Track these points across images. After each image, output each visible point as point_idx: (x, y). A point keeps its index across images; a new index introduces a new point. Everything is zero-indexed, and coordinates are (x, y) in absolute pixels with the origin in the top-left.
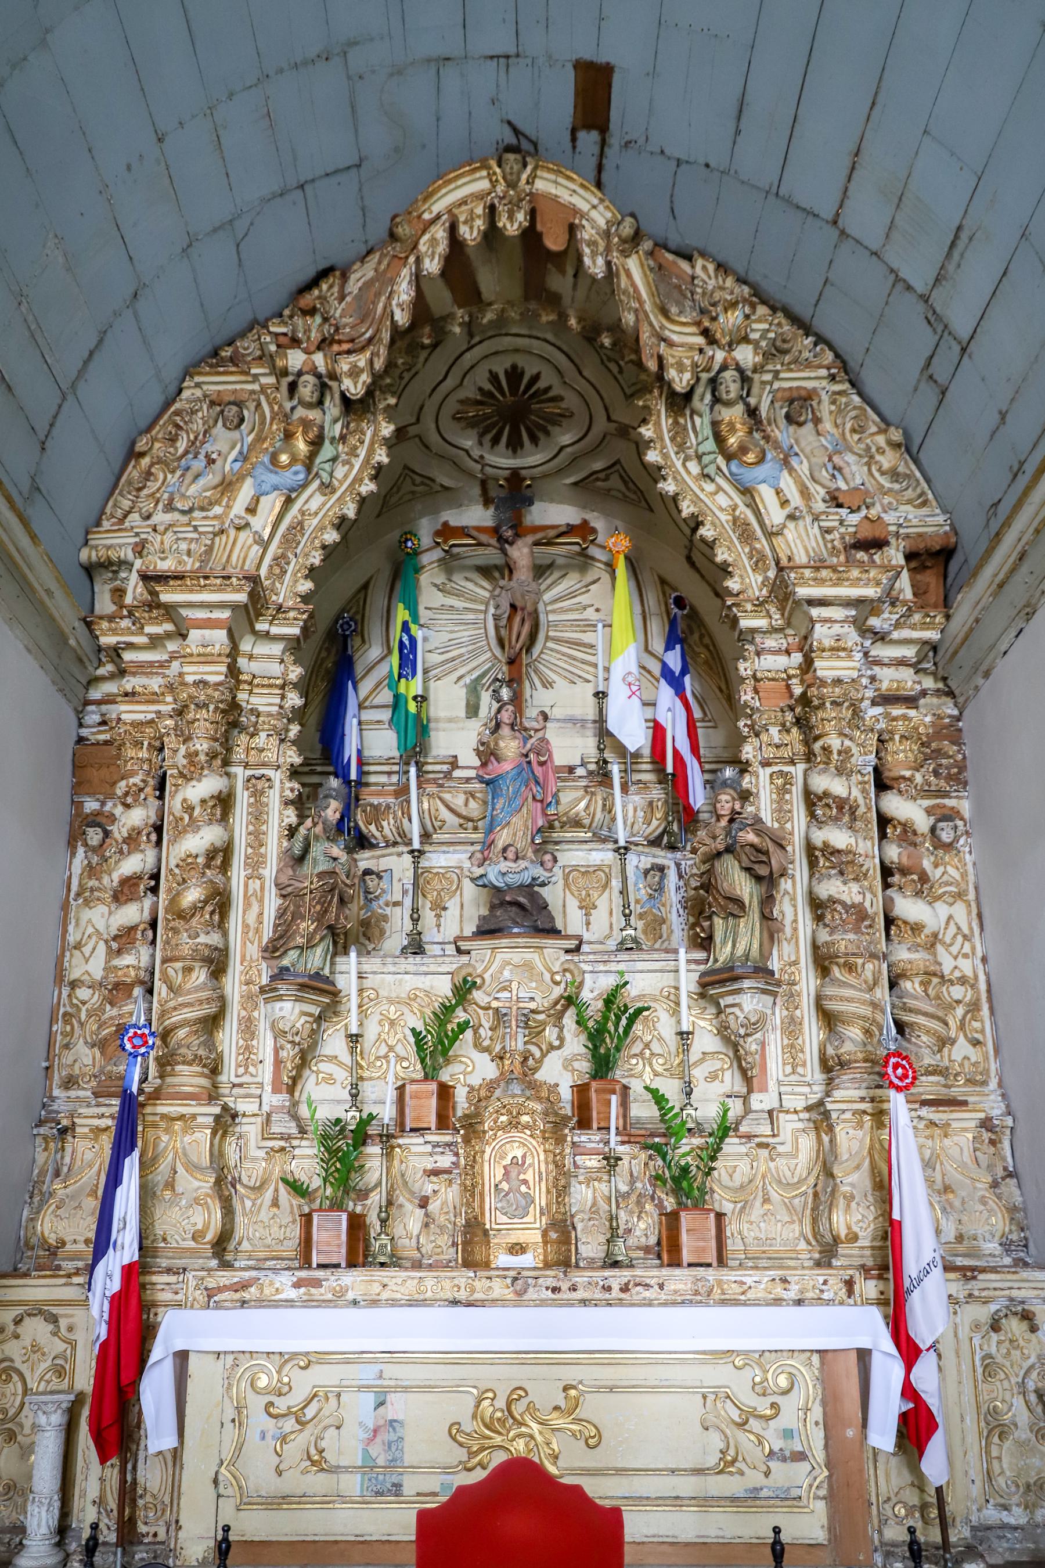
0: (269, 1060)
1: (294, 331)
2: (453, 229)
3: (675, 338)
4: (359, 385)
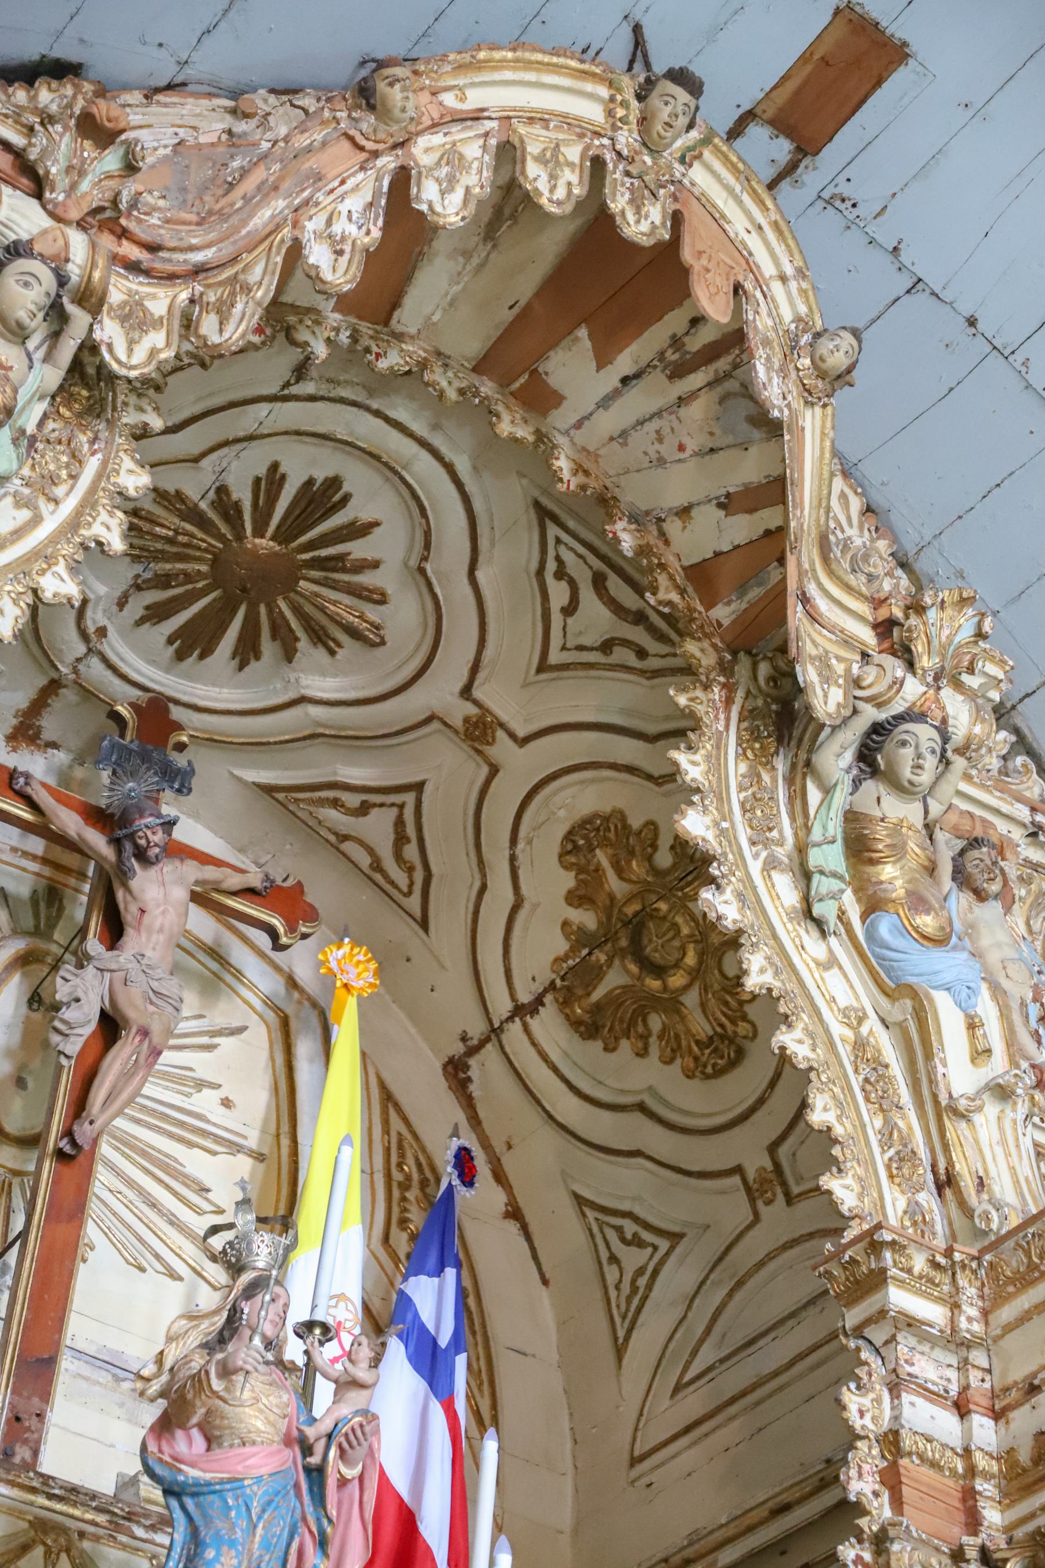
1: (44, 153)
3: (822, 605)
4: (140, 355)
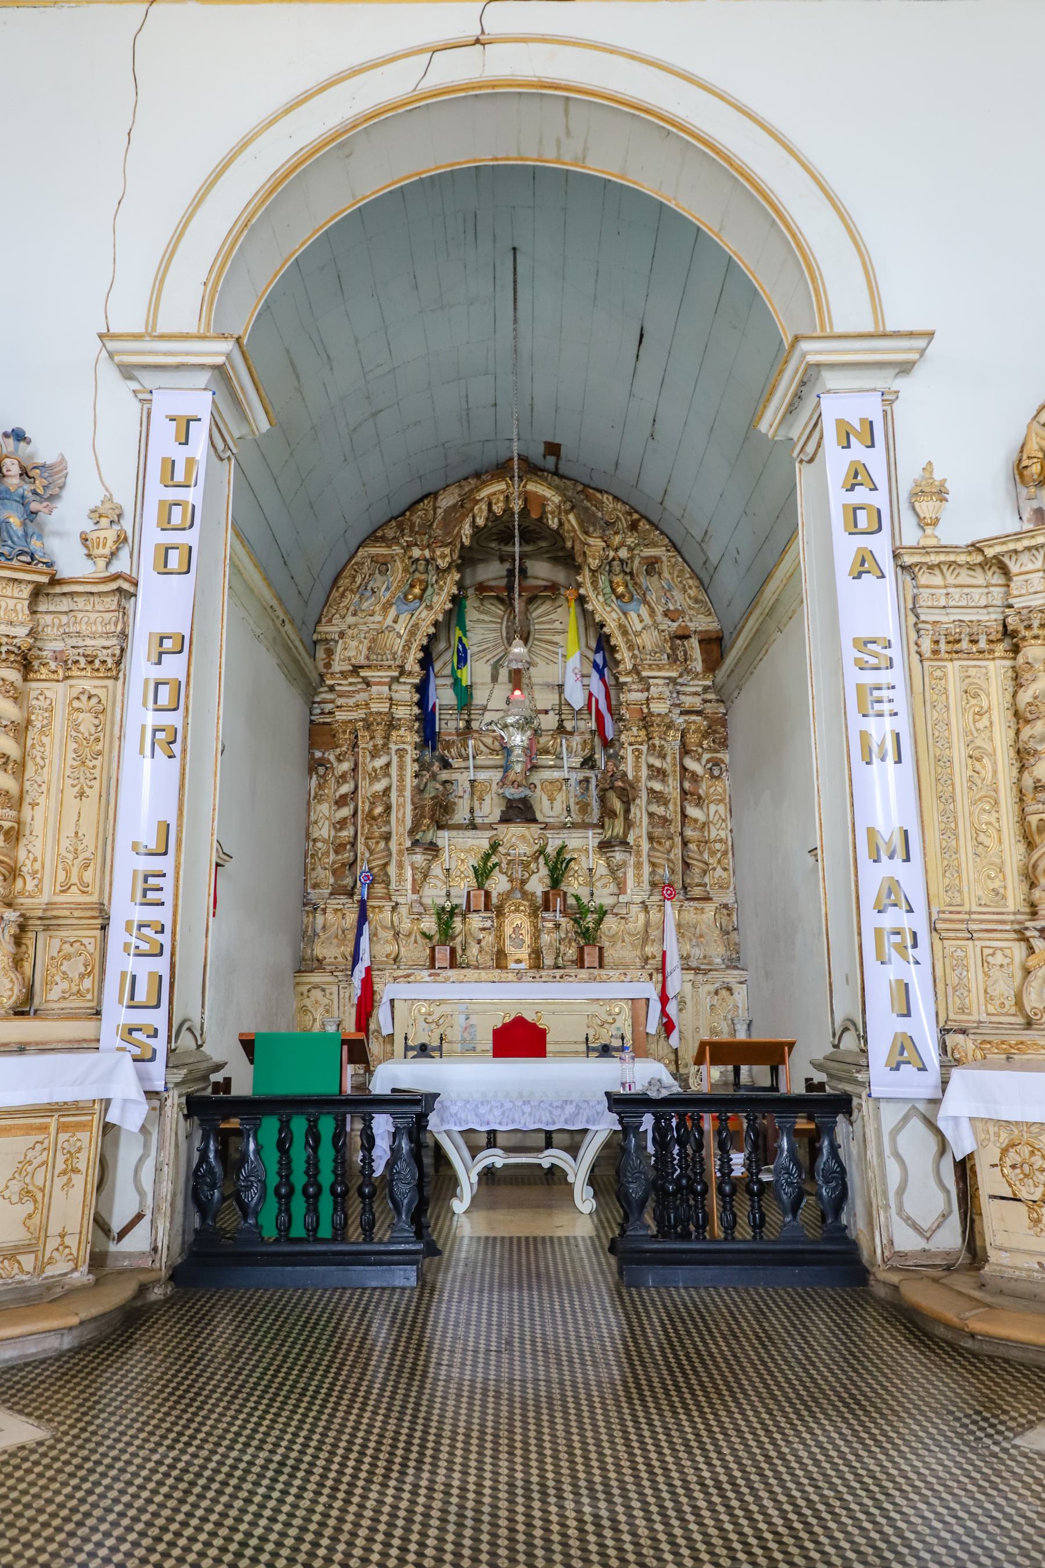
0: (410, 880)
2: (490, 505)
